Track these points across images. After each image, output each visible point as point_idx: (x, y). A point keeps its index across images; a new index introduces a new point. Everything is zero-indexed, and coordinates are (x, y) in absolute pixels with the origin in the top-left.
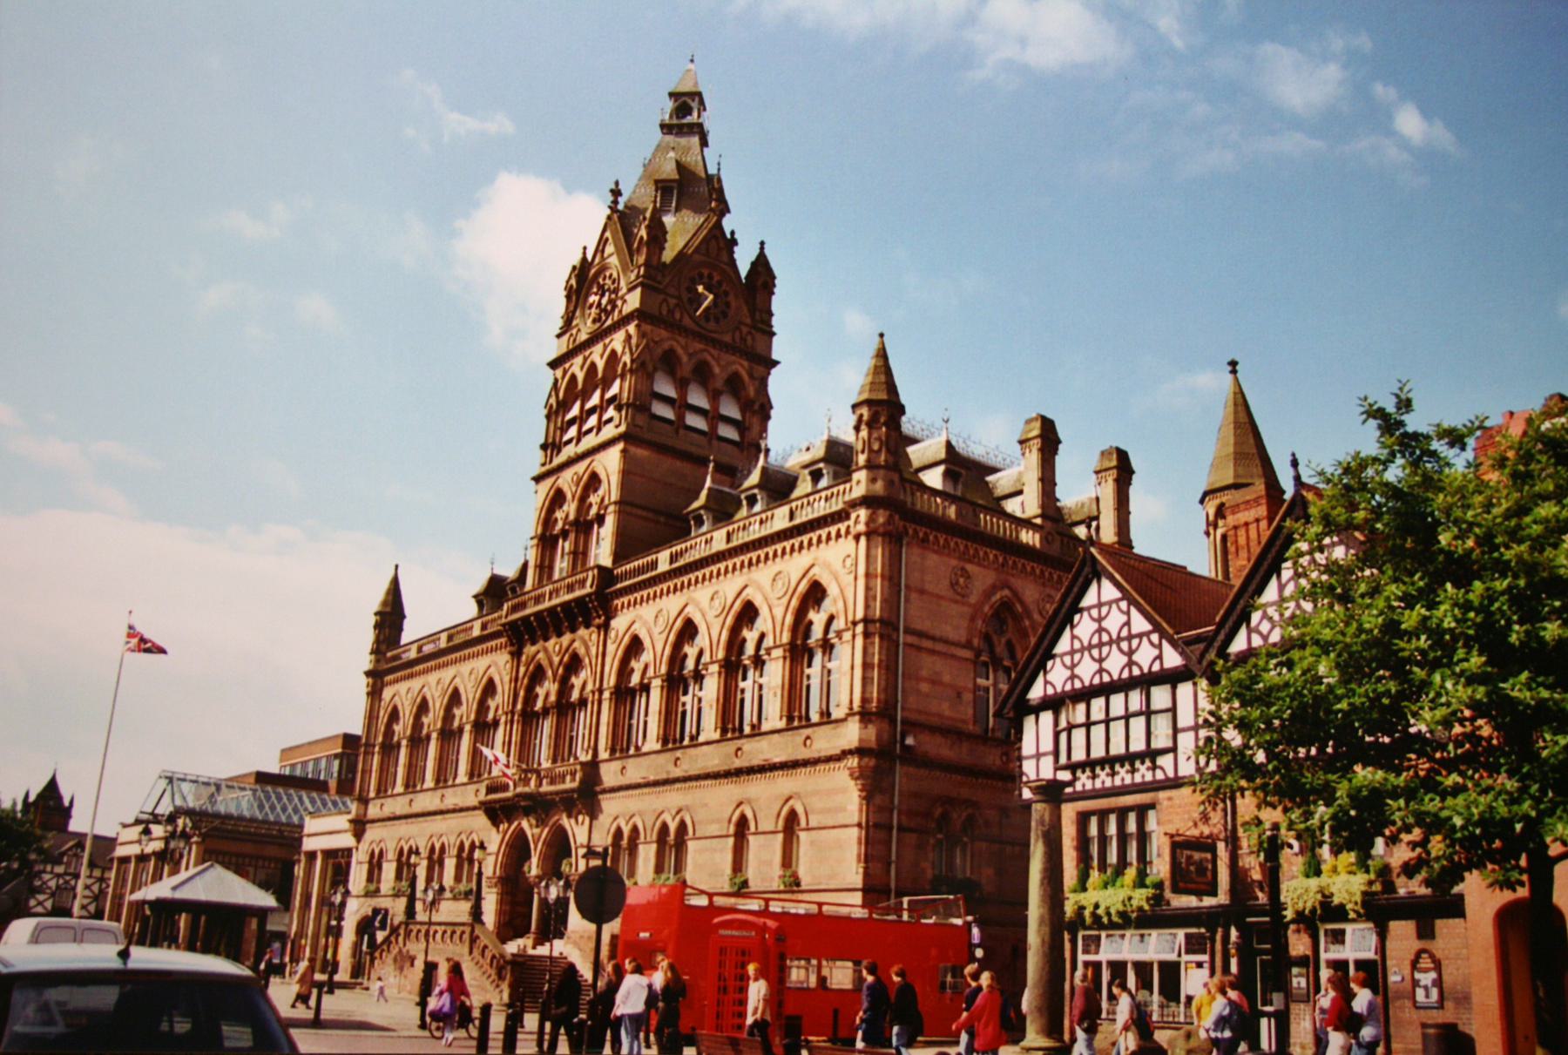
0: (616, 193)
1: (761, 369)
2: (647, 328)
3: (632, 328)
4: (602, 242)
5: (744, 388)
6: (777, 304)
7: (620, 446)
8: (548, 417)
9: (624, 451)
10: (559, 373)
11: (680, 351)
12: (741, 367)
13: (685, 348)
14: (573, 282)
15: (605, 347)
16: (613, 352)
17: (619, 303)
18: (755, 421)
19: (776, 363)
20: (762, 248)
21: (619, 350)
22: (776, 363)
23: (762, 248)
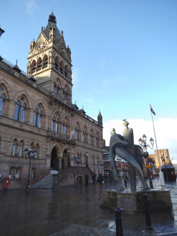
0: (42, 28)
1: (70, 67)
2: (54, 50)
3: (51, 50)
4: (40, 37)
5: (68, 69)
6: (71, 56)
7: (51, 70)
8: (28, 68)
9: (51, 71)
10: (30, 60)
11: (59, 57)
12: (68, 65)
13: (60, 57)
14: (32, 44)
15: (43, 54)
16: (46, 55)
17: (46, 46)
18: (70, 75)
19: (72, 66)
20: (68, 46)
21: (48, 54)
22: (72, 66)
23: (68, 46)
